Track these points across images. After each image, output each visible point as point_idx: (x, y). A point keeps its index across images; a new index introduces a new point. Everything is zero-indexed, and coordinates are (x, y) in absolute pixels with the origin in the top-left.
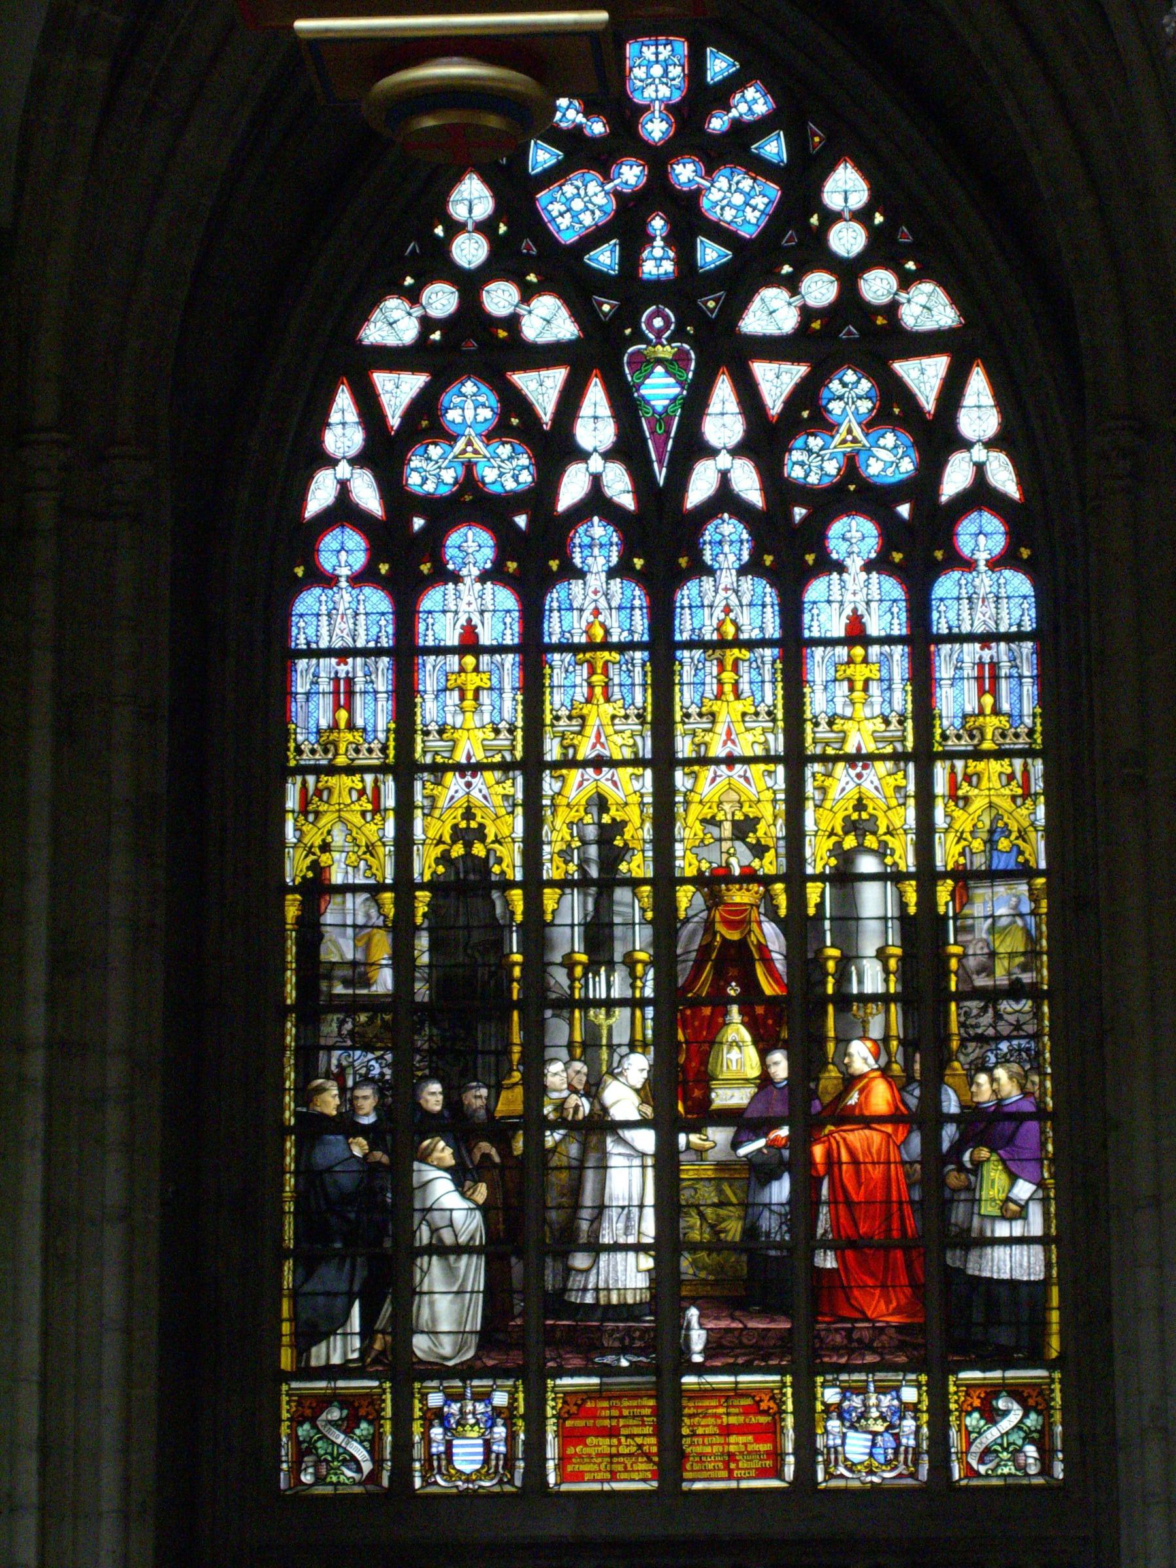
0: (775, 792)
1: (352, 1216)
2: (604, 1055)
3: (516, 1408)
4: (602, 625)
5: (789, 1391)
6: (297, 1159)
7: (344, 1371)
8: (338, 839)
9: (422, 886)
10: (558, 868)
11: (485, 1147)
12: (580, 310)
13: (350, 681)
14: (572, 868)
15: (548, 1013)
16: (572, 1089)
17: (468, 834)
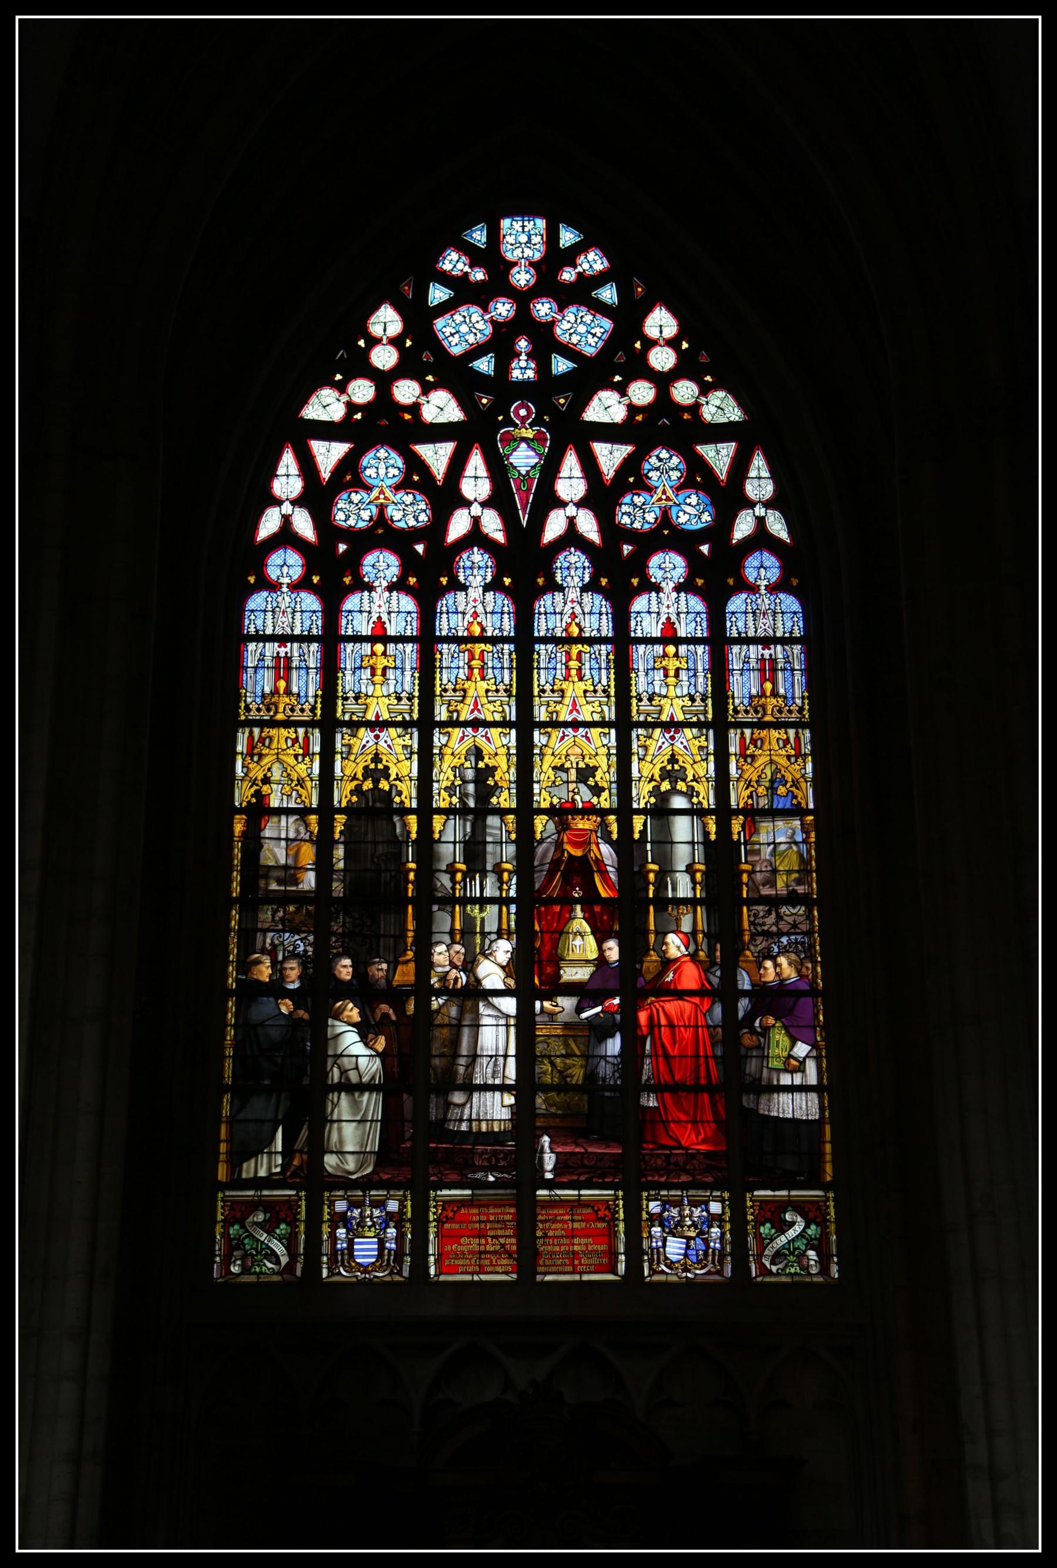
0: (608, 749)
1: (279, 1060)
2: (478, 940)
3: (405, 1213)
4: (480, 624)
5: (621, 1202)
6: (237, 1015)
7: (269, 1182)
8: (276, 774)
9: (340, 811)
10: (444, 800)
11: (385, 1008)
13: (288, 659)
14: (455, 800)
15: (435, 908)
16: (453, 965)
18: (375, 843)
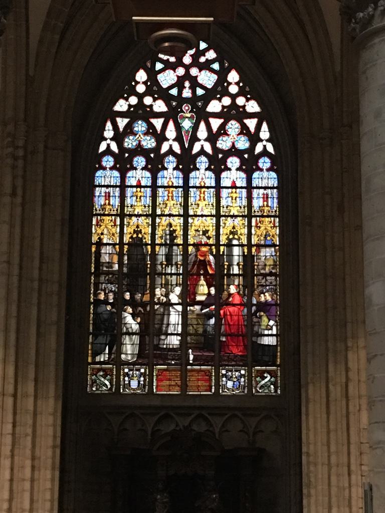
1: (107, 325)
2: (170, 287)
5: (213, 370)
6: (93, 310)
7: (104, 363)
8: (105, 232)
9: (126, 244)
11: (140, 309)
12: (168, 104)
13: (109, 193)
14: (163, 241)
15: (156, 276)
16: (162, 295)
17: (137, 232)
18: (137, 255)
